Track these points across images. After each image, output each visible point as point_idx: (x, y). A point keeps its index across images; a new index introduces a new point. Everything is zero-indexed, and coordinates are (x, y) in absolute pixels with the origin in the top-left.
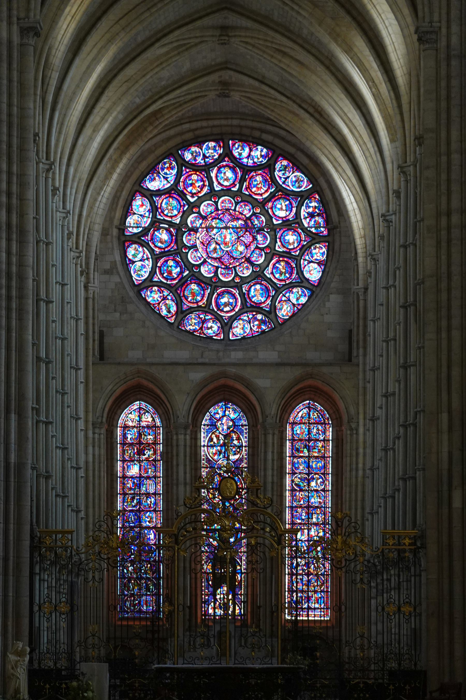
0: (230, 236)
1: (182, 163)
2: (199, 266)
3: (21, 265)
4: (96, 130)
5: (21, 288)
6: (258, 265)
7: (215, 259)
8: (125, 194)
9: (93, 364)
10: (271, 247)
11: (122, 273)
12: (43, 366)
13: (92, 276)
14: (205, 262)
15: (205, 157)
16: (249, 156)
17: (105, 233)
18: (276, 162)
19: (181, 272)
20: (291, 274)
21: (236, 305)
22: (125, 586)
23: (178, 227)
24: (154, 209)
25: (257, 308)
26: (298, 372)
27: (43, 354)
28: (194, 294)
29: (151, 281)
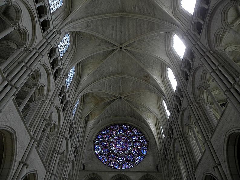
2: (113, 150)
6: (129, 150)
7: (118, 148)
8: (96, 134)
9: (80, 171)
11: (93, 151)
13: (84, 147)
14: (115, 149)
15: (116, 127)
16: (126, 127)
17: (90, 141)
18: (133, 128)
19: (109, 151)
20: (138, 152)
21: (124, 160)
23: (108, 141)
24: (103, 138)
25: (130, 161)
26: (143, 174)
28: (112, 157)
29: (100, 153)
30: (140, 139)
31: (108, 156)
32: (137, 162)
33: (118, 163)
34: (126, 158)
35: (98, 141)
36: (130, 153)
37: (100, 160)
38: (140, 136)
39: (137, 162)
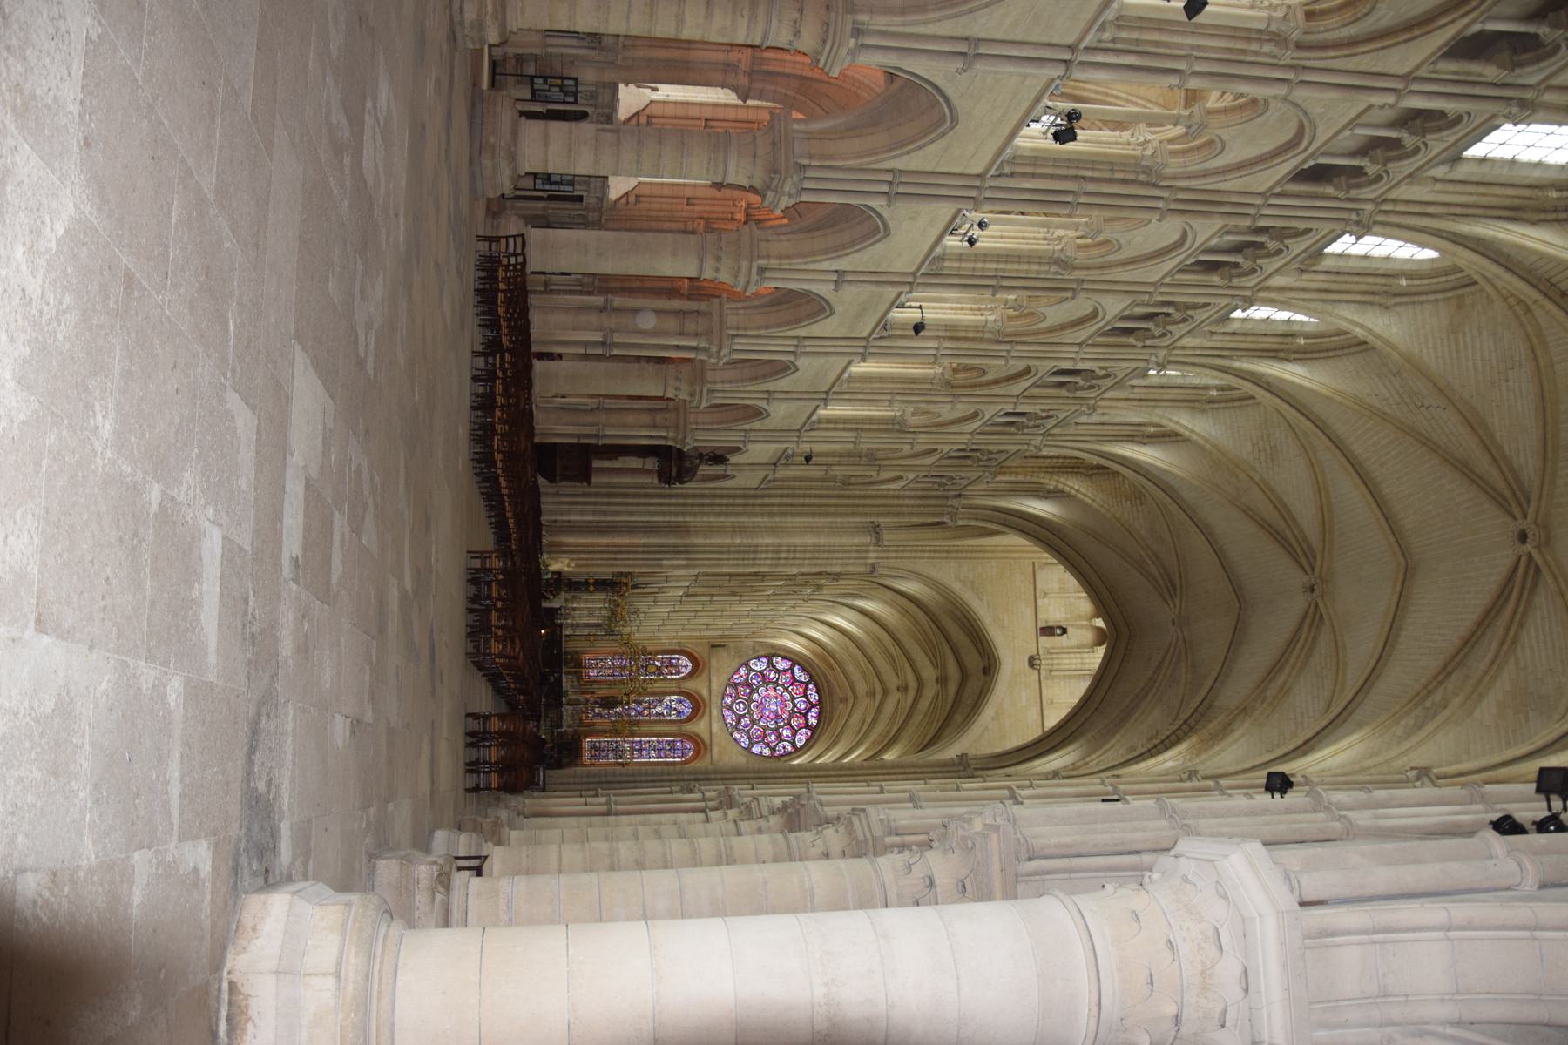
0: (773, 707)
1: (807, 684)
3: (759, 565)
4: (823, 633)
5: (748, 565)
8: (792, 657)
10: (768, 728)
12: (709, 599)
17: (773, 646)
22: (601, 660)
24: (785, 671)
25: (739, 722)
26: (707, 740)
27: (715, 599)
28: (744, 691)
30: (786, 744)
31: (747, 684)
32: (737, 735)
33: (733, 702)
34: (743, 716)
35: (777, 663)
36: (753, 722)
37: (737, 671)
38: (793, 744)
39: (737, 735)
